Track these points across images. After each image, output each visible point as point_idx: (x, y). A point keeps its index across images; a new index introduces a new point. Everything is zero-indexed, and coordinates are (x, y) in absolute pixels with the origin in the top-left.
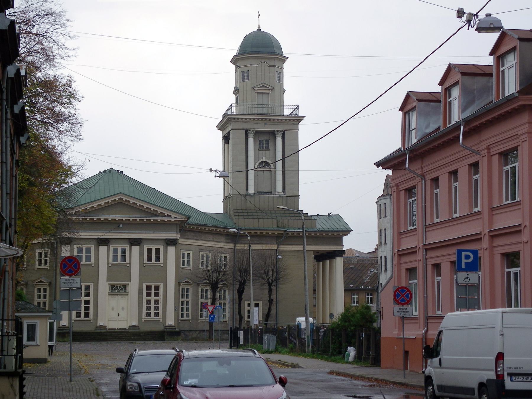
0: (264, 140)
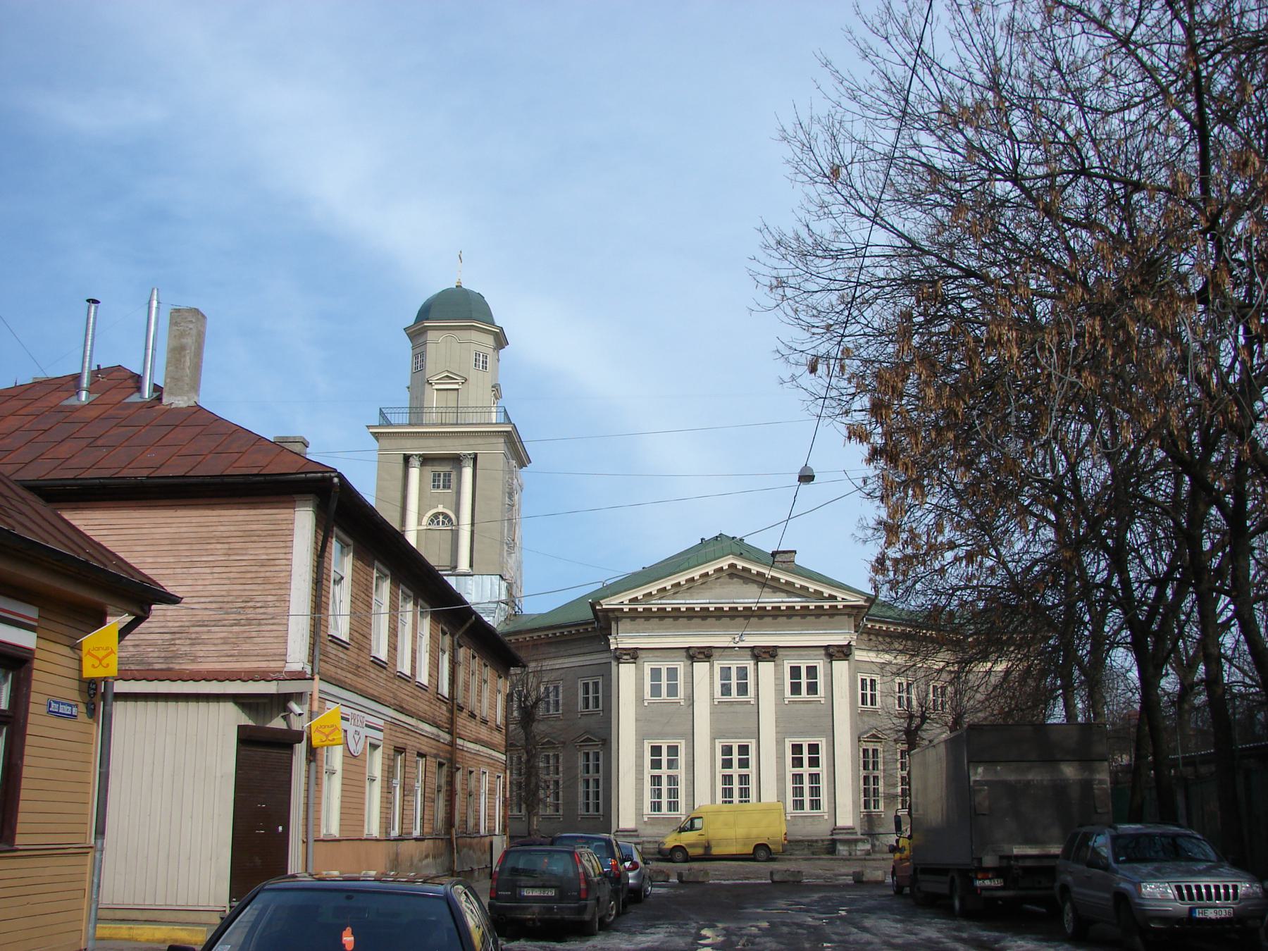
0: (442, 473)
